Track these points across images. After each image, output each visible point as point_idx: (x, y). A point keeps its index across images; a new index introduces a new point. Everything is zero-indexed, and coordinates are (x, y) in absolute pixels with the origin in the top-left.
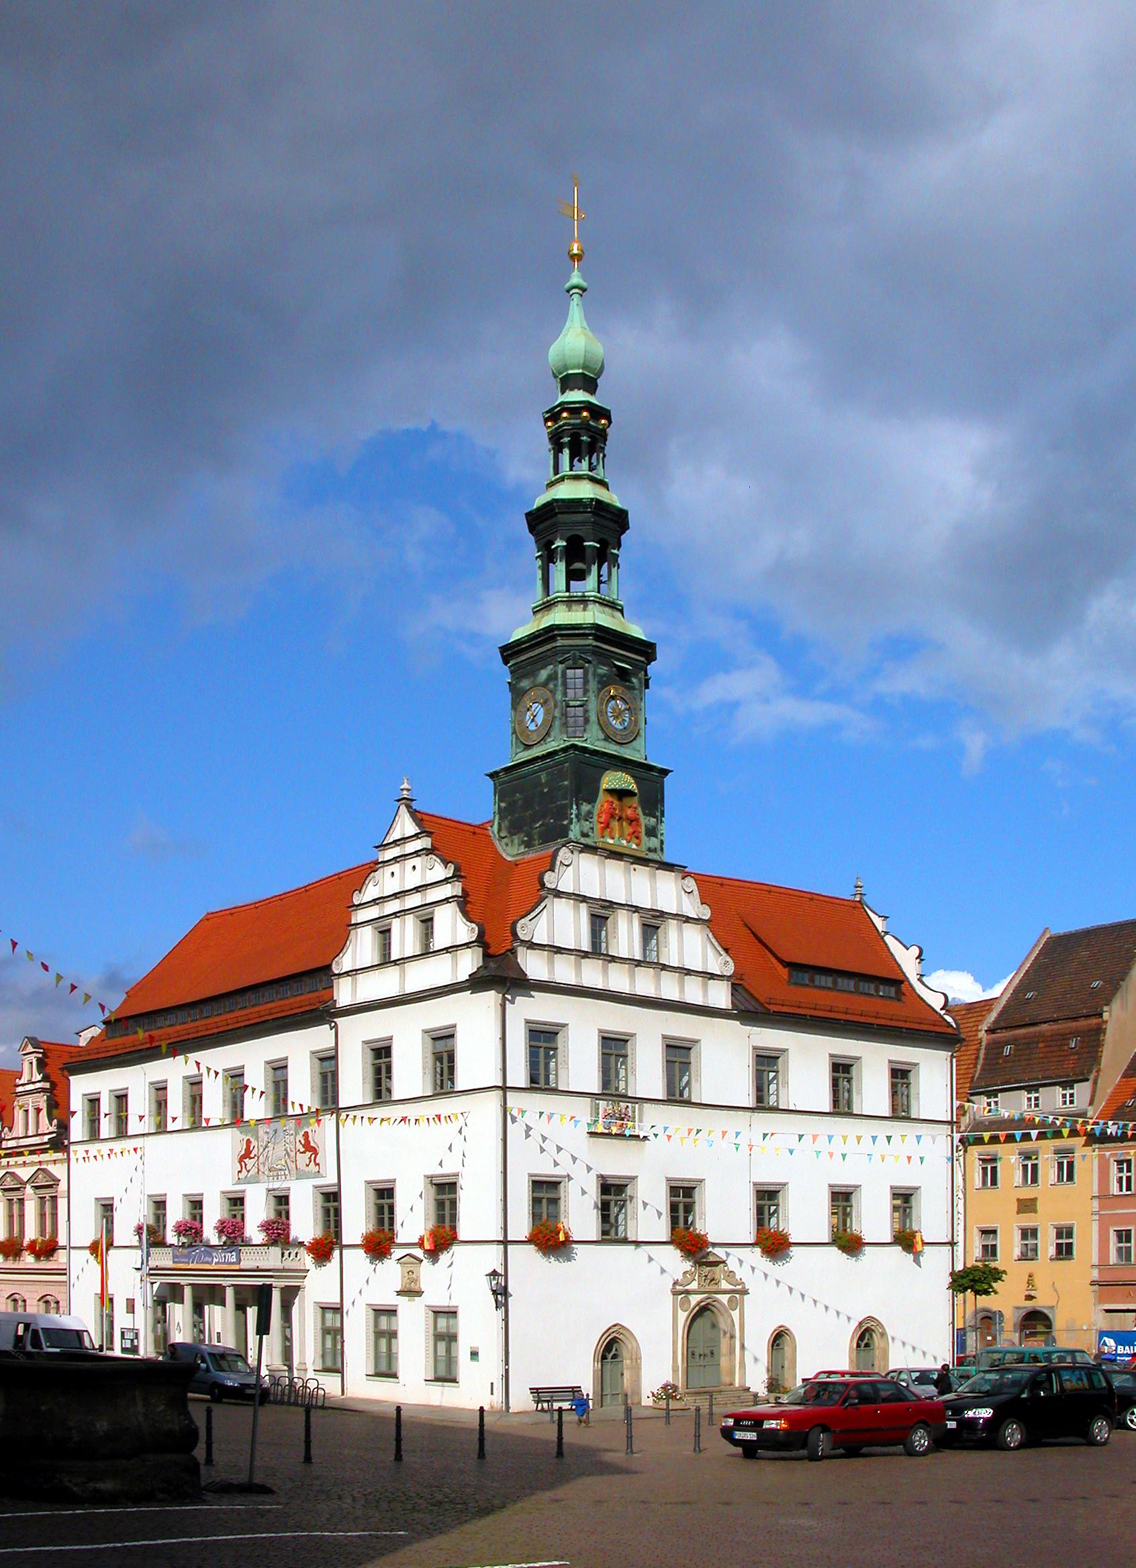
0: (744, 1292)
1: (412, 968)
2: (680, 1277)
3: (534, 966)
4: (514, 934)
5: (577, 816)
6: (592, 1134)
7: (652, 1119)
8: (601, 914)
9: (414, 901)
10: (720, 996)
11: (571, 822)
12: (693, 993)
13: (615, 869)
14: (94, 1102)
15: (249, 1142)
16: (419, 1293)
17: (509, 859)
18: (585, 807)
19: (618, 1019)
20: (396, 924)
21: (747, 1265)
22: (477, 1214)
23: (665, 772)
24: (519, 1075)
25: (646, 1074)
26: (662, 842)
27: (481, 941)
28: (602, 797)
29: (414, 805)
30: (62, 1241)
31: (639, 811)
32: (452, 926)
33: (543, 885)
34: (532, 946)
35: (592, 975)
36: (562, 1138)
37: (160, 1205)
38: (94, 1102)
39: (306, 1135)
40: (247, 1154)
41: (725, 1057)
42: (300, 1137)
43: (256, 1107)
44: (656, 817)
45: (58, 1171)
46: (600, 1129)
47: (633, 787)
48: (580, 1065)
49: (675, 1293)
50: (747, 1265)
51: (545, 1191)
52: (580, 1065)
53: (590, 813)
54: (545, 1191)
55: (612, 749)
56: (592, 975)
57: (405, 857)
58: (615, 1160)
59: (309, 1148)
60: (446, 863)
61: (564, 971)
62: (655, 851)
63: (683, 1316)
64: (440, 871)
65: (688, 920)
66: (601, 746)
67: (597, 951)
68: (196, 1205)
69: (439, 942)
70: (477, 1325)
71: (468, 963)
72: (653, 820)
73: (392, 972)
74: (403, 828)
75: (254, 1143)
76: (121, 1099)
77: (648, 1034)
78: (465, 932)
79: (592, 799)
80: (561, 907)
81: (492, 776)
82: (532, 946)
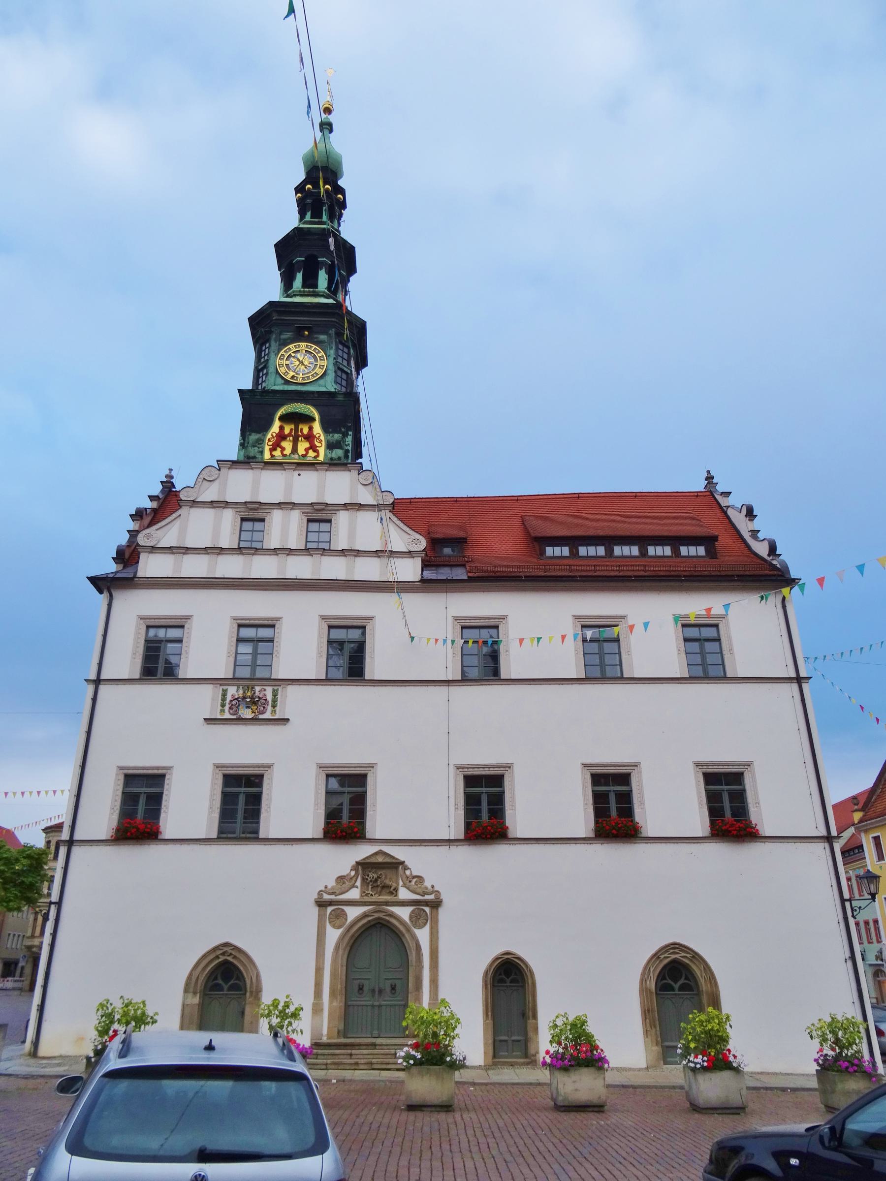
0: (436, 904)
2: (331, 883)
8: (253, 514)
19: (257, 605)
26: (347, 451)
28: (275, 428)
35: (231, 567)
46: (227, 715)
48: (208, 651)
49: (321, 904)
50: (451, 871)
52: (208, 651)
58: (245, 746)
61: (195, 567)
63: (333, 935)
65: (360, 507)
66: (280, 387)
67: (247, 549)
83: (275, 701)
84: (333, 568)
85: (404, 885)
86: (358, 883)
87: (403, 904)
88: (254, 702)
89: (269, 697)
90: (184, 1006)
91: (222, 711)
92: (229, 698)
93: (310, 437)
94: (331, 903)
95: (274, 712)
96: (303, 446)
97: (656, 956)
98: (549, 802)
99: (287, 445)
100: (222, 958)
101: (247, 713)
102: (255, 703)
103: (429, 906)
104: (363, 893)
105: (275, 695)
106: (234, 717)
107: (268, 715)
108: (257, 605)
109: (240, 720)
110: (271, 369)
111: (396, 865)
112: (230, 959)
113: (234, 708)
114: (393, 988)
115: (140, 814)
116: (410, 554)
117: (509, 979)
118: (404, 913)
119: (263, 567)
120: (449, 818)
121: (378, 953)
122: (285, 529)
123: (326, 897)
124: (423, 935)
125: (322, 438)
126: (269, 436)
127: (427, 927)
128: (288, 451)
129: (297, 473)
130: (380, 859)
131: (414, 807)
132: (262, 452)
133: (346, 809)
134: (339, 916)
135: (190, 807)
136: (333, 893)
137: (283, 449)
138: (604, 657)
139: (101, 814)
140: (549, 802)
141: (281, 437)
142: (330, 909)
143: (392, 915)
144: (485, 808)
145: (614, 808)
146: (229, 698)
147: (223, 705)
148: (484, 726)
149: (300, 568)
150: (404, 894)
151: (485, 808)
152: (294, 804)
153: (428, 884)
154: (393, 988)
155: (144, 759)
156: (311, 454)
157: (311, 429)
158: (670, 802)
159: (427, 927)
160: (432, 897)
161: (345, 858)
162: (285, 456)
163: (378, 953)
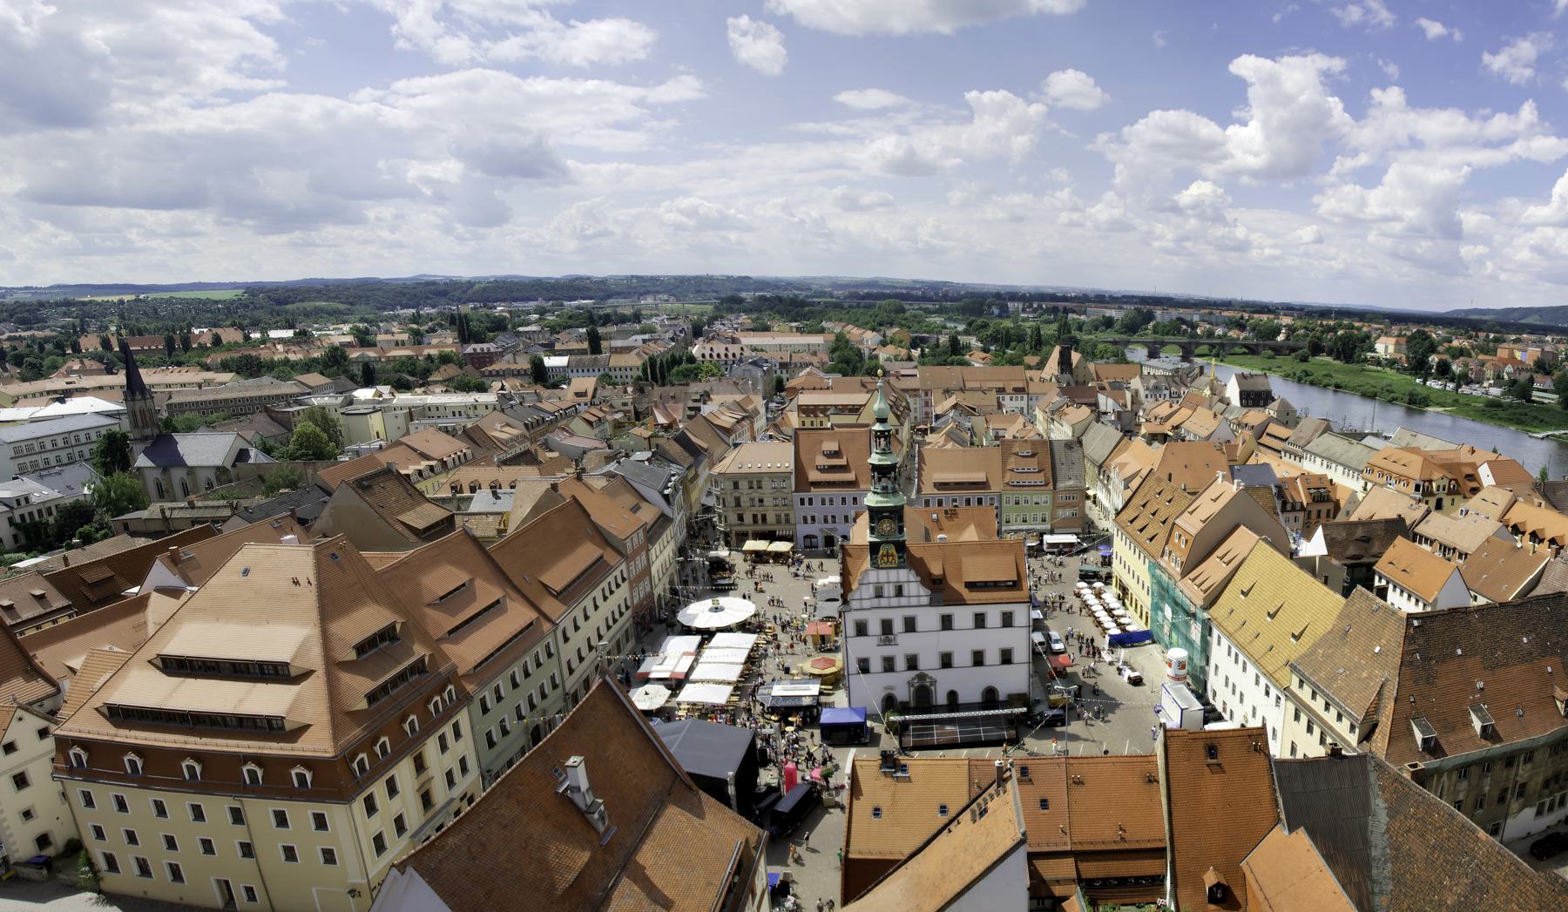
10: (925, 600)
12: (914, 601)
25: (898, 626)
41: (929, 618)
56: (875, 602)
58: (888, 651)
61: (866, 604)
98: (962, 658)
103: (934, 682)
108: (886, 614)
115: (864, 667)
120: (937, 662)
133: (912, 663)
135: (876, 665)
138: (980, 621)
139: (854, 667)
140: (962, 658)
144: (946, 661)
145: (978, 659)
148: (947, 641)
151: (946, 661)
152: (900, 664)
158: (992, 657)
161: (913, 673)
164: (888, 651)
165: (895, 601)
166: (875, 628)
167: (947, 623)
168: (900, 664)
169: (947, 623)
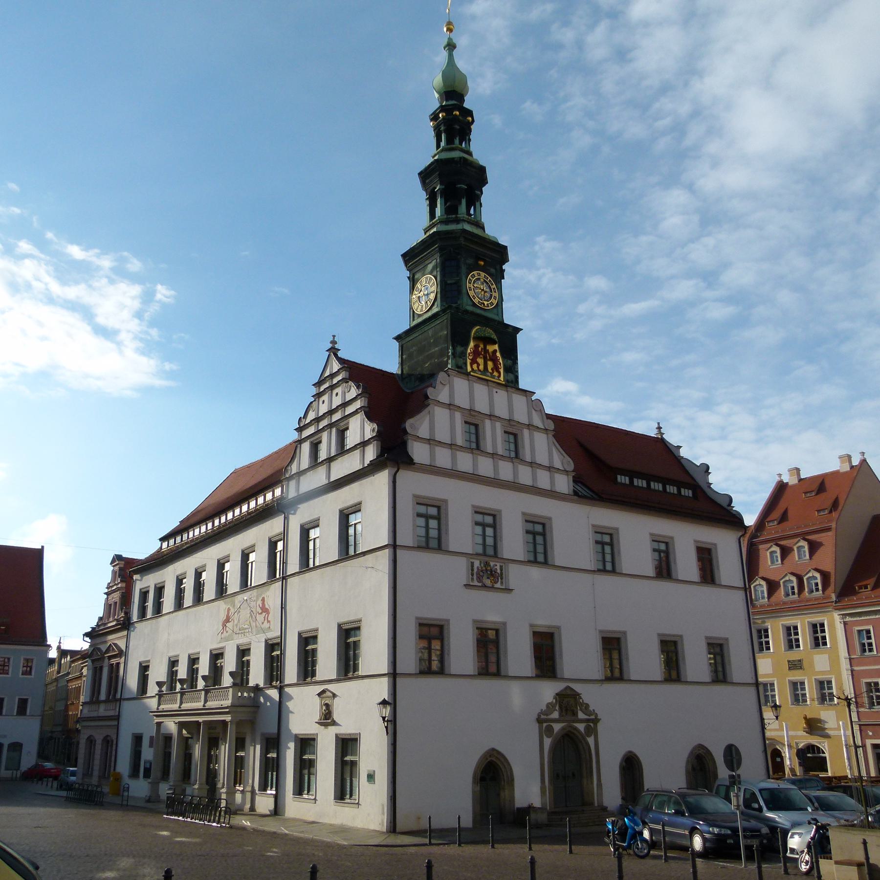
0: (596, 721)
1: (334, 465)
2: (544, 708)
3: (418, 452)
4: (405, 432)
5: (453, 354)
6: (467, 586)
7: (516, 575)
9: (336, 417)
10: (564, 484)
11: (448, 359)
12: (543, 480)
13: (481, 390)
14: (144, 594)
15: (229, 610)
16: (334, 723)
17: (408, 391)
18: (459, 349)
19: (489, 498)
20: (325, 436)
21: (596, 697)
22: (374, 653)
23: (518, 330)
24: (406, 537)
27: (380, 436)
28: (472, 344)
29: (340, 354)
30: (118, 696)
31: (498, 354)
32: (360, 429)
33: (427, 397)
34: (418, 438)
35: (465, 462)
36: (446, 589)
37: (173, 663)
38: (144, 594)
39: (263, 600)
40: (227, 620)
42: (260, 602)
43: (233, 582)
44: (510, 359)
45: (122, 645)
47: (494, 337)
49: (539, 721)
51: (433, 633)
53: (463, 355)
54: (433, 633)
55: (478, 311)
56: (465, 462)
57: (332, 387)
58: (490, 608)
59: (265, 610)
60: (358, 387)
61: (443, 458)
62: (512, 382)
63: (548, 742)
64: (353, 392)
68: (193, 661)
69: (350, 442)
70: (373, 755)
71: (371, 453)
72: (509, 362)
73: (322, 471)
74: (332, 368)
75: (232, 611)
76: (160, 590)
77: (513, 510)
78: (370, 429)
79: (467, 344)
80: (441, 415)
81: (398, 338)
82: (418, 438)
83: (502, 574)
84: (525, 476)
85: (581, 710)
86: (557, 708)
87: (581, 721)
88: (493, 575)
89: (499, 571)
90: (474, 792)
91: (472, 579)
92: (475, 570)
93: (494, 360)
94: (546, 721)
95: (502, 583)
96: (490, 365)
97: (691, 753)
99: (480, 361)
100: (489, 759)
101: (488, 582)
102: (492, 575)
103: (593, 722)
104: (560, 715)
105: (501, 570)
106: (480, 584)
107: (498, 585)
108: (489, 498)
109: (484, 586)
110: (464, 291)
111: (576, 696)
112: (494, 759)
113: (479, 579)
114: (574, 775)
116: (566, 472)
117: (631, 767)
118: (581, 727)
119: (485, 466)
121: (570, 754)
122: (494, 437)
123: (542, 717)
124: (591, 740)
125: (501, 361)
126: (469, 351)
127: (593, 737)
128: (481, 367)
129: (495, 390)
130: (569, 692)
131: (580, 658)
132: (466, 364)
134: (549, 730)
135: (462, 652)
136: (547, 715)
137: (478, 365)
141: (476, 353)
142: (545, 725)
143: (576, 729)
146: (475, 570)
147: (472, 575)
149: (506, 471)
150: (581, 715)
153: (591, 709)
154: (574, 775)
155: (433, 613)
156: (496, 374)
157: (495, 351)
159: (593, 737)
160: (593, 717)
161: (548, 691)
162: (480, 370)
163: (570, 754)
164: (490, 608)
165: (506, 471)
166: (462, 533)
167: (607, 553)
168: (519, 654)
169: (607, 553)
